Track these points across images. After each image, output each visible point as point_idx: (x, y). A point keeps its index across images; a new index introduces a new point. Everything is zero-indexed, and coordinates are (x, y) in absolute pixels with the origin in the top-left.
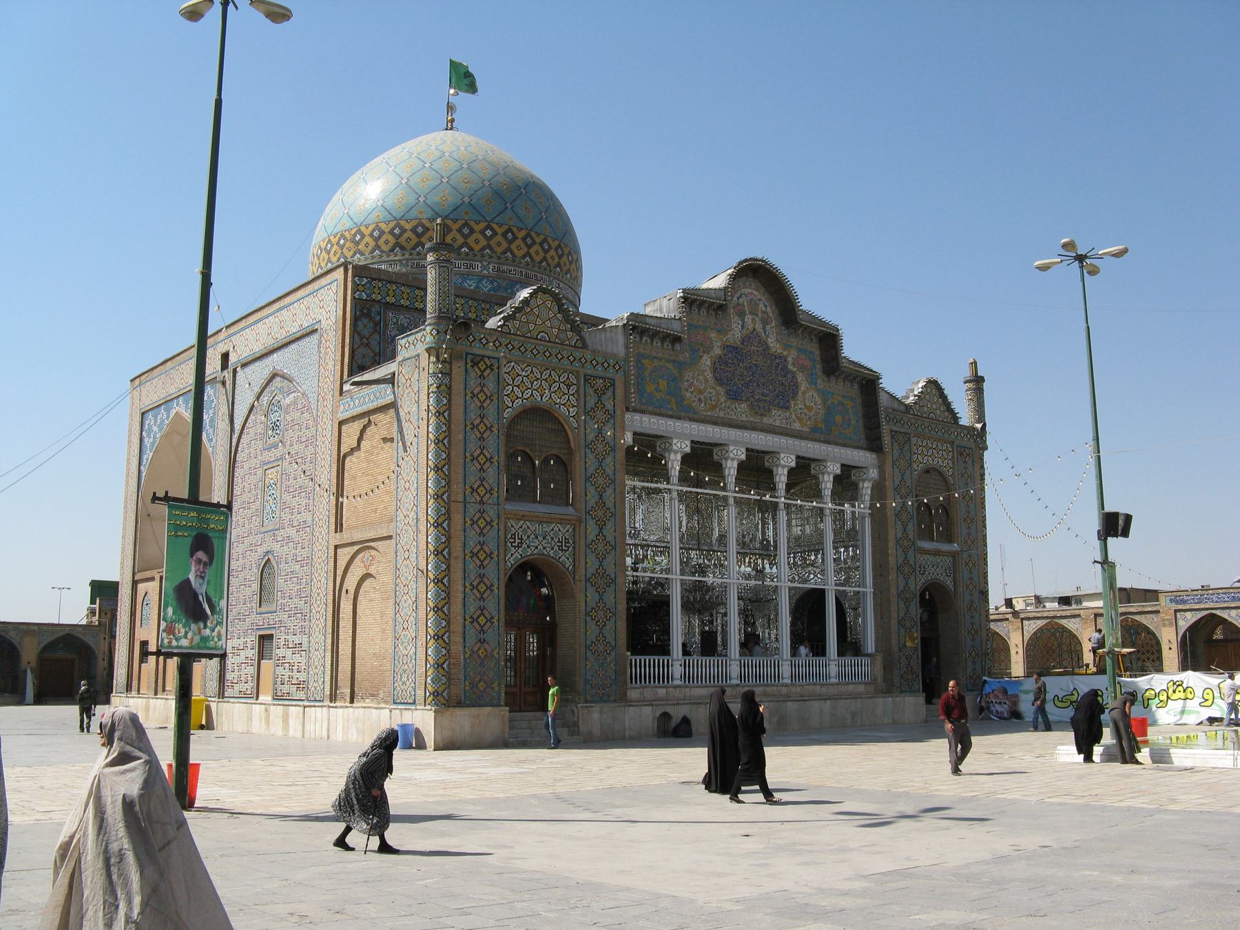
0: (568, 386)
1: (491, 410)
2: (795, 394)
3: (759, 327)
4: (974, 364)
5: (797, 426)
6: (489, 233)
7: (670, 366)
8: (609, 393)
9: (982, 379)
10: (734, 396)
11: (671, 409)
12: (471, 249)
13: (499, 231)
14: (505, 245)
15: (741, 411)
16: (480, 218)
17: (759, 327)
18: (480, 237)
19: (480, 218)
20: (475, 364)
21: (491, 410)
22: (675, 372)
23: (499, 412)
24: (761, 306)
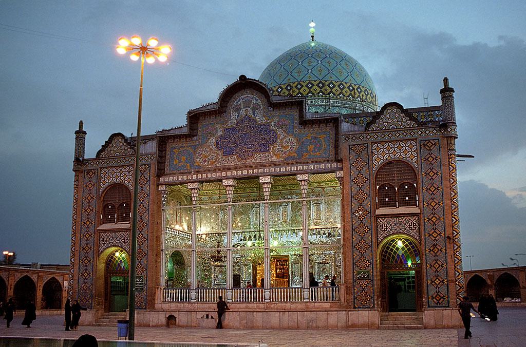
0: (129, 172)
1: (94, 191)
2: (274, 142)
3: (250, 113)
4: (446, 80)
5: (274, 159)
7: (189, 149)
8: (148, 171)
9: (452, 90)
10: (228, 153)
13: (304, 84)
14: (308, 90)
15: (233, 160)
16: (317, 79)
17: (250, 113)
18: (306, 88)
19: (317, 79)
21: (94, 191)
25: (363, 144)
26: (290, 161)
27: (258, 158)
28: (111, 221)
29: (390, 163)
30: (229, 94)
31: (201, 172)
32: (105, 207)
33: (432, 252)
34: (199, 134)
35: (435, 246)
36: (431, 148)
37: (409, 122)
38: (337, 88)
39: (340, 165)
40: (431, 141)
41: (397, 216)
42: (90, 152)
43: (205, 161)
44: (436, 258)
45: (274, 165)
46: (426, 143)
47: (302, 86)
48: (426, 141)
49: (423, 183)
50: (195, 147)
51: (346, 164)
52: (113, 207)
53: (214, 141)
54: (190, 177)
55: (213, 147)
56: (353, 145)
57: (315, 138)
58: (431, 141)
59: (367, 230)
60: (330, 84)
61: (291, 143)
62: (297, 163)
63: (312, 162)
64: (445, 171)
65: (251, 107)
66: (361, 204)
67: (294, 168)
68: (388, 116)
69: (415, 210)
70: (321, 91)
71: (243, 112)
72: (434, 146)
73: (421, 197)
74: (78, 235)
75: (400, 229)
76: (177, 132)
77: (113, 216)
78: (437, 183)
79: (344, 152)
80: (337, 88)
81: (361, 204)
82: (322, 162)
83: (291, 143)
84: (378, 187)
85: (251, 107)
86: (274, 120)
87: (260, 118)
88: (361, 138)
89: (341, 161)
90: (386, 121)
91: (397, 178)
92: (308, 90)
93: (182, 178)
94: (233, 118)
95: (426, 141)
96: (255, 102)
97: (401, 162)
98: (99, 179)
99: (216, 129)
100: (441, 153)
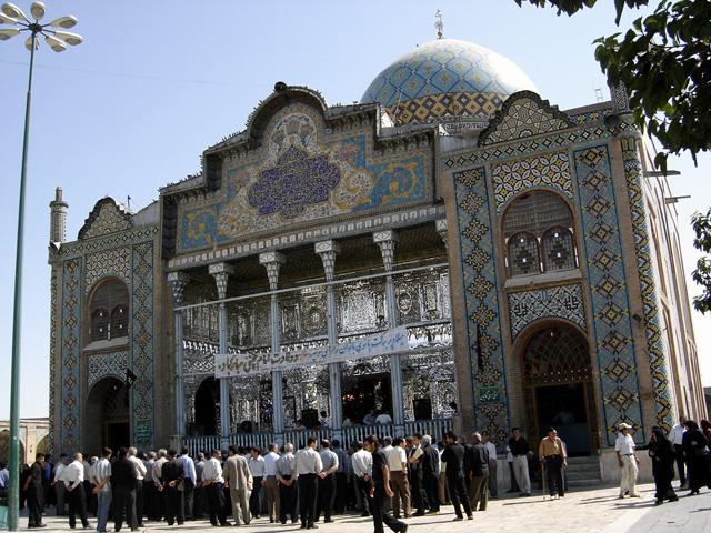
1: (77, 289)
2: (335, 184)
3: (297, 142)
5: (337, 211)
6: (413, 107)
8: (149, 252)
10: (266, 211)
11: (207, 243)
12: (470, 113)
13: (420, 103)
14: (427, 112)
15: (274, 221)
17: (297, 142)
18: (424, 109)
20: (69, 265)
22: (213, 213)
23: (82, 290)
24: (304, 122)
25: (477, 169)
26: (361, 213)
27: (311, 213)
28: (102, 337)
29: (525, 196)
30: (263, 117)
31: (226, 246)
32: (95, 315)
33: (608, 347)
34: (224, 185)
35: (612, 334)
36: (595, 162)
37: (553, 122)
38: (473, 103)
39: (441, 209)
40: (594, 150)
41: (544, 287)
42: (70, 234)
43: (233, 227)
44: (616, 356)
45: (339, 220)
46: (584, 154)
47: (418, 106)
48: (584, 150)
49: (584, 223)
50: (218, 207)
51: (450, 206)
52: (105, 314)
53: (245, 194)
54: (211, 255)
55: (245, 204)
56: (462, 173)
57: (400, 169)
58: (594, 150)
59: (491, 315)
60: (461, 97)
61: (363, 182)
62: (372, 215)
63: (397, 210)
64: (622, 199)
65: (299, 131)
66: (479, 273)
67: (368, 223)
68: (516, 116)
69: (576, 274)
70: (448, 111)
71: (286, 142)
72: (598, 158)
73: (582, 250)
74: (58, 362)
75: (550, 311)
76: (190, 186)
77: (105, 330)
78: (609, 222)
79: (446, 184)
80: (473, 103)
81: (479, 273)
82: (413, 207)
83: (363, 182)
84: (507, 240)
85: (299, 131)
86: (332, 149)
87: (313, 149)
88: (474, 158)
89: (439, 202)
90: (513, 125)
91: (537, 217)
92: (427, 112)
93: (201, 259)
94: (271, 154)
95: (584, 150)
96: (304, 123)
97: (544, 194)
98: (84, 272)
99: (248, 174)
100: (613, 168)
